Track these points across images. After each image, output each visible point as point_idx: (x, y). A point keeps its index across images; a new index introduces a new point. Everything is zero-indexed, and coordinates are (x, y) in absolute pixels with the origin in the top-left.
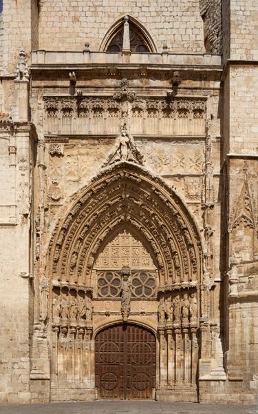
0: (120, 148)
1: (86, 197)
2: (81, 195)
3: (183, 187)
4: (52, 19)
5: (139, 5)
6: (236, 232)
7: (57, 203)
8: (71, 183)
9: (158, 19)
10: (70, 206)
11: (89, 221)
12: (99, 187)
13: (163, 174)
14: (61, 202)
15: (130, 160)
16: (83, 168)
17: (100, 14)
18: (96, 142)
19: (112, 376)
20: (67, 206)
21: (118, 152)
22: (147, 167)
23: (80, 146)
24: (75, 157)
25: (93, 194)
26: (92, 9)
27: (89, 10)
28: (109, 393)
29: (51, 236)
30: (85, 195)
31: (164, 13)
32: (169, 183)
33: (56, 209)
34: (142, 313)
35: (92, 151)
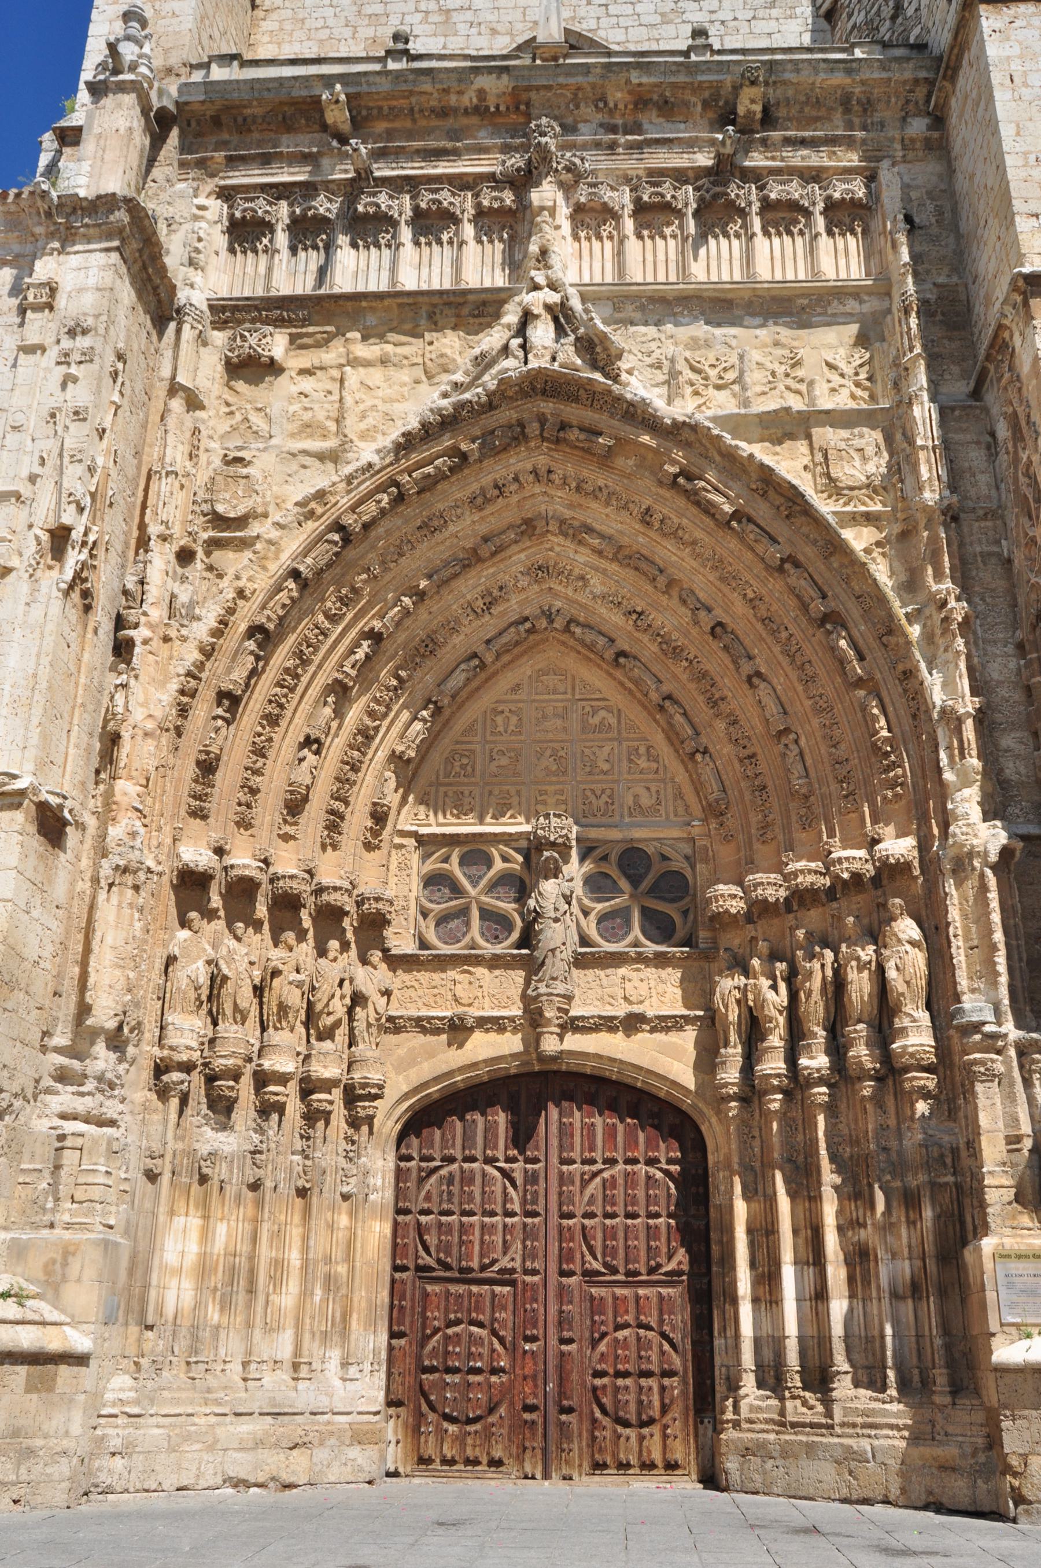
0: (521, 330)
1: (370, 510)
2: (345, 501)
3: (806, 460)
8: (308, 461)
10: (292, 544)
12: (429, 469)
13: (709, 413)
14: (255, 528)
16: (362, 407)
17: (462, 28)
19: (480, 1341)
21: (515, 342)
24: (336, 373)
25: (400, 499)
26: (435, 18)
27: (425, 21)
28: (460, 1440)
30: (361, 502)
33: (231, 555)
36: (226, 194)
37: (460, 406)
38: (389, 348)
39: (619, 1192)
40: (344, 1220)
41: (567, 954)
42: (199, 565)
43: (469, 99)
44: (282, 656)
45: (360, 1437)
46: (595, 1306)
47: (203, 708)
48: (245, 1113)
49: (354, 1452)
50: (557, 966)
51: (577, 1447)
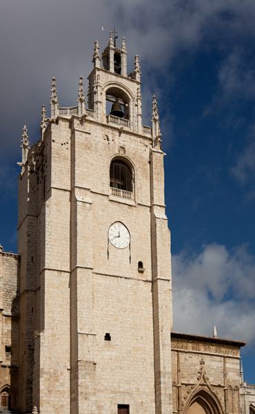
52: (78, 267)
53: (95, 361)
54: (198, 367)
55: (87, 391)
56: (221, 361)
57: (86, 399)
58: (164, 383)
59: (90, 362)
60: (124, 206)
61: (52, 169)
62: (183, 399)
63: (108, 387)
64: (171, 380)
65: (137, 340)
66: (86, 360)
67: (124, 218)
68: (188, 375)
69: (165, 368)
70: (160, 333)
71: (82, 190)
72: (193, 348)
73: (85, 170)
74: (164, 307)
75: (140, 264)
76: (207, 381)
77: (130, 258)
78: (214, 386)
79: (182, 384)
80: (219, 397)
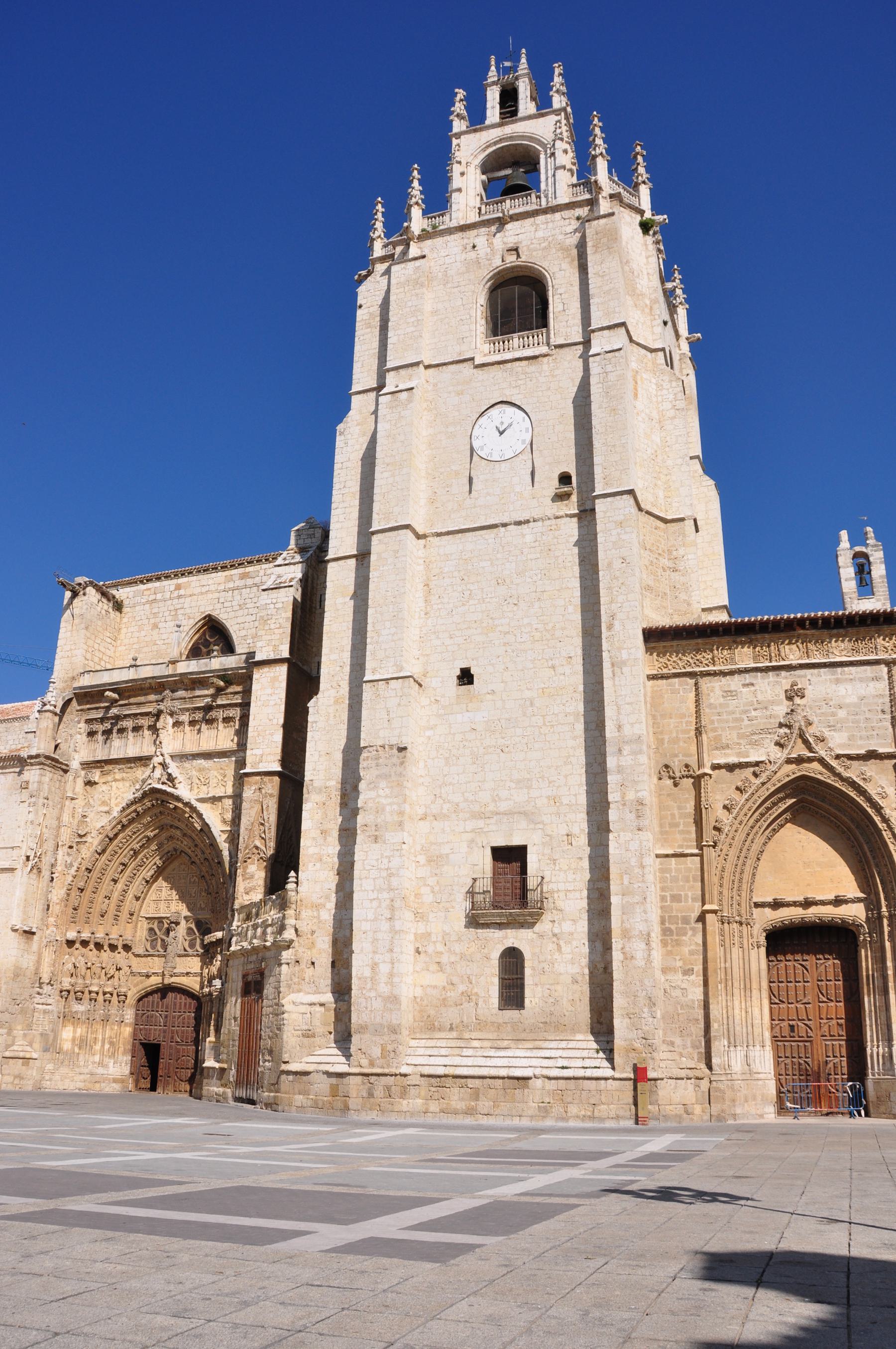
1: (116, 831)
2: (109, 828)
4: (132, 629)
5: (222, 600)
6: (247, 867)
7: (84, 839)
9: (240, 613)
10: (96, 842)
11: (125, 856)
14: (89, 839)
15: (163, 783)
17: (180, 617)
18: (133, 765)
20: (94, 841)
22: (183, 791)
23: (116, 771)
25: (123, 826)
29: (71, 879)
31: (248, 606)
32: (202, 808)
34: (188, 974)
35: (128, 775)
36: (89, 721)
37: (135, 798)
38: (124, 775)
39: (186, 1020)
40: (116, 1027)
41: (172, 954)
42: (74, 849)
43: (147, 685)
44: (95, 874)
45: (115, 1081)
46: (178, 1051)
47: (74, 893)
48: (86, 1000)
49: (114, 1085)
50: (170, 958)
51: (171, 1087)
52: (373, 533)
53: (405, 741)
54: (781, 709)
55: (379, 820)
56: (876, 679)
57: (376, 839)
58: (620, 770)
59: (391, 747)
60: (518, 363)
61: (355, 359)
62: (721, 814)
63: (462, 805)
64: (643, 759)
65: (553, 667)
66: (381, 744)
67: (516, 391)
68: (740, 736)
69: (619, 728)
70: (604, 636)
71: (402, 372)
72: (755, 659)
73: (413, 329)
74: (617, 564)
75: (565, 479)
76: (817, 748)
77: (533, 474)
78: (850, 757)
79: (715, 767)
80: (872, 790)
